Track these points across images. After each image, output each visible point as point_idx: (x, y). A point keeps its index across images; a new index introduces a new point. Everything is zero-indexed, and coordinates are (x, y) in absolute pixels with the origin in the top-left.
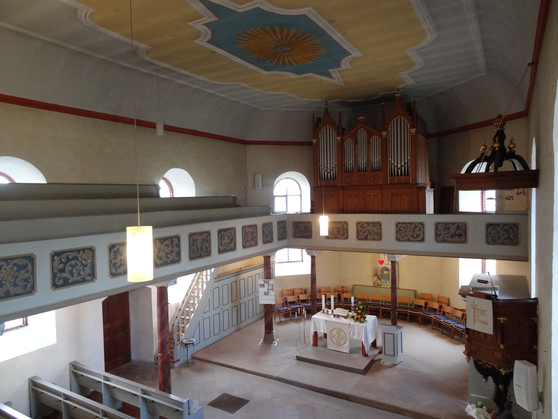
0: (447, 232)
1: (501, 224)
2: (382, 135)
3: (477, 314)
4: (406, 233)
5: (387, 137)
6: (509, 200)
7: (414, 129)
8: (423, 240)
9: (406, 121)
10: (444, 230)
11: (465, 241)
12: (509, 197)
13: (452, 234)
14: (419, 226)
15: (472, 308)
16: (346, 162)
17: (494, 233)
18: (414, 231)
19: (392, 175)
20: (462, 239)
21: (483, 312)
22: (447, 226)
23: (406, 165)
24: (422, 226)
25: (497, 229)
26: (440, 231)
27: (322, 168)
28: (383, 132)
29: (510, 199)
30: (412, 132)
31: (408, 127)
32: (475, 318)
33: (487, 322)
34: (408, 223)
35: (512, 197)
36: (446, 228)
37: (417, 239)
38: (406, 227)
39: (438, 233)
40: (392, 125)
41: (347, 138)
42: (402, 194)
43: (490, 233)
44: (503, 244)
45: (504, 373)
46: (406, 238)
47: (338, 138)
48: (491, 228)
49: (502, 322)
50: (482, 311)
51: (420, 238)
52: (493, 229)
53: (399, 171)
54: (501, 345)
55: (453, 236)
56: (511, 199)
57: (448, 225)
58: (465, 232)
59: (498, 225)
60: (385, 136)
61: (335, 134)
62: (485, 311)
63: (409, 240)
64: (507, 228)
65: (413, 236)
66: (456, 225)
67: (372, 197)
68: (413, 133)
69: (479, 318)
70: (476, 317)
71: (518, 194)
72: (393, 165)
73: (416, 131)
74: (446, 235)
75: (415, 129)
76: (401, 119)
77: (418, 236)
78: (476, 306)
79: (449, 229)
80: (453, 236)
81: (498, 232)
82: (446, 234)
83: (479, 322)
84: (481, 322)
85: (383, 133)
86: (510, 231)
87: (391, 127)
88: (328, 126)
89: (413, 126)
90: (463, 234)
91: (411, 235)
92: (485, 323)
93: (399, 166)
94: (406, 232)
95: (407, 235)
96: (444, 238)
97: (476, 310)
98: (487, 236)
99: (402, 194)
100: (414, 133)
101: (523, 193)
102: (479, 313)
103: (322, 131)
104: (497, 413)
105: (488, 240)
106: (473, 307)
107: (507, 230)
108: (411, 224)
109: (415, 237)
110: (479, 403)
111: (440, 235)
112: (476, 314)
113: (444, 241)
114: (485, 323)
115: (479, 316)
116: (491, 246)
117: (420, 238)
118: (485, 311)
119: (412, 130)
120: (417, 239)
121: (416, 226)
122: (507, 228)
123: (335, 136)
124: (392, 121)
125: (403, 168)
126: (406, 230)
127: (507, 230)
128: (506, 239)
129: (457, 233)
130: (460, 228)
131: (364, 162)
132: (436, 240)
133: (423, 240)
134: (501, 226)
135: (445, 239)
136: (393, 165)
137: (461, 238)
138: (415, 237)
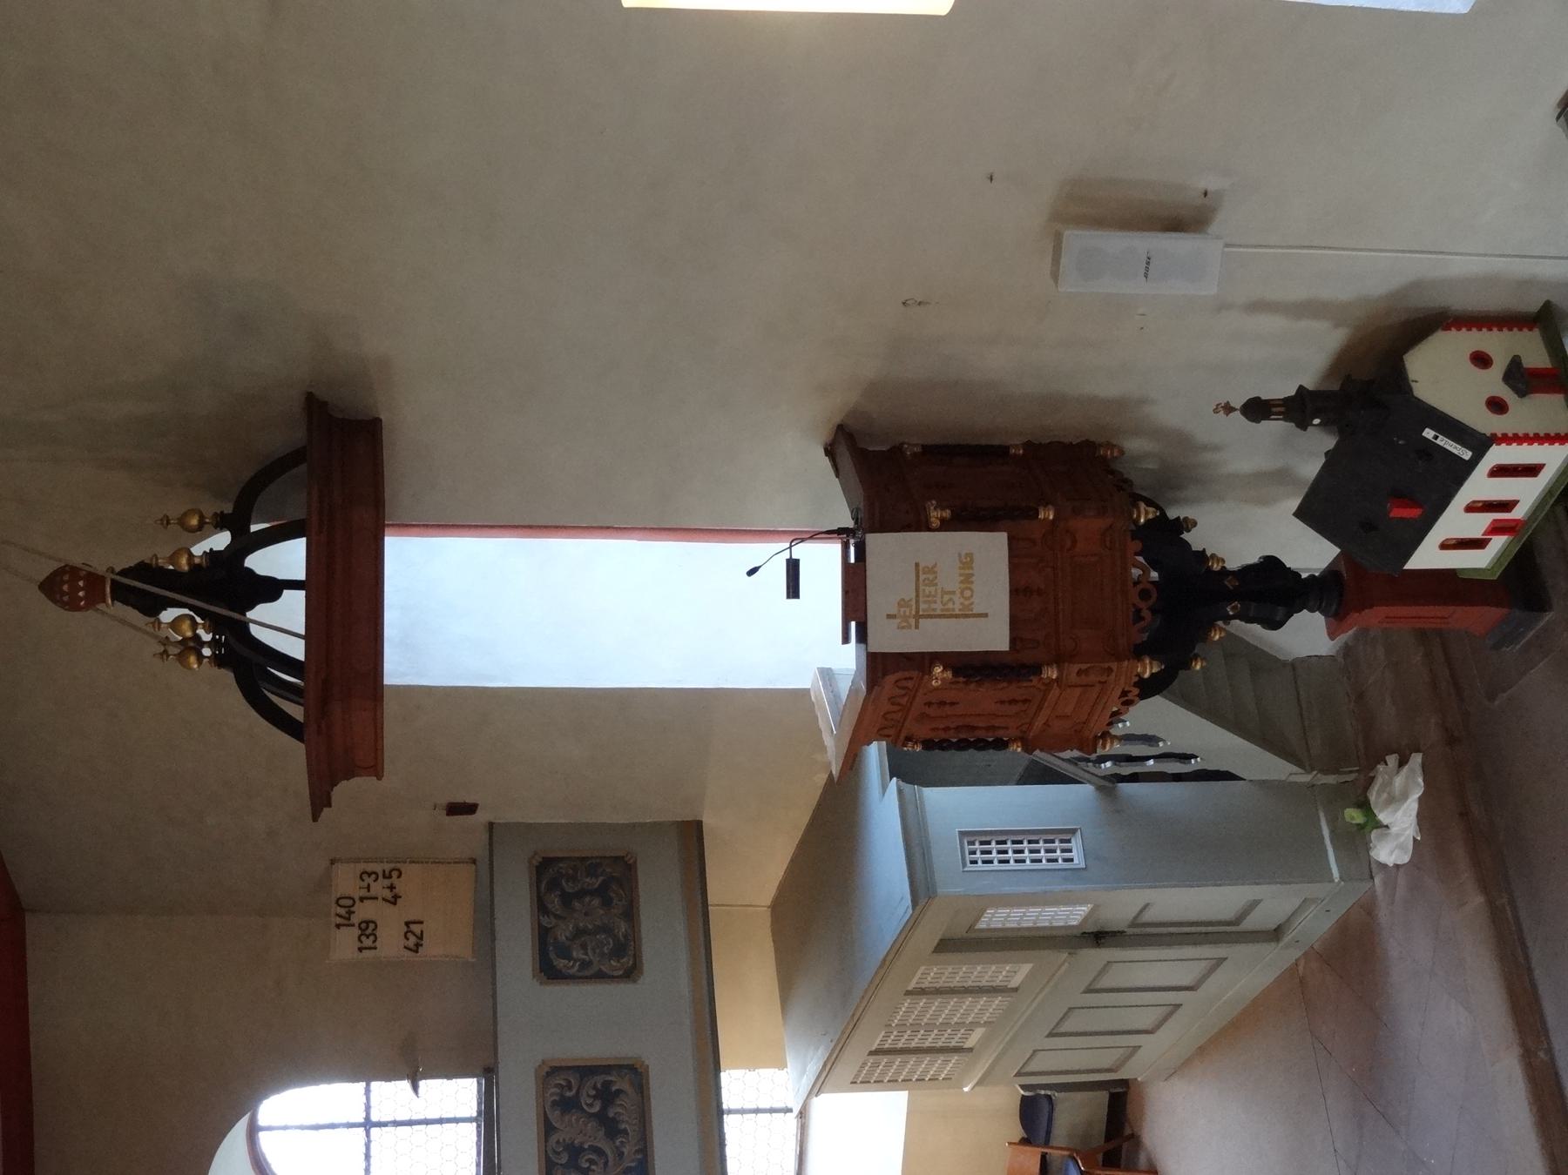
1: (540, 925)
6: (421, 938)
11: (636, 1073)
13: (601, 1133)
15: (917, 627)
17: (584, 947)
21: (923, 574)
22: (564, 1159)
29: (419, 933)
32: (957, 612)
33: (960, 555)
35: (407, 924)
43: (585, 965)
44: (631, 914)
45: (1151, 509)
48: (560, 963)
49: (947, 514)
50: (922, 577)
52: (565, 953)
54: (1041, 516)
55: (612, 1129)
56: (416, 928)
57: (558, 1153)
58: (586, 1071)
59: (543, 937)
62: (917, 565)
64: (554, 902)
66: (554, 1116)
69: (954, 593)
70: (950, 605)
71: (394, 900)
78: (903, 603)
79: (575, 1151)
80: (612, 1129)
81: (579, 933)
82: (606, 1163)
83: (968, 593)
84: (967, 579)
86: (569, 888)
90: (599, 1080)
92: (967, 562)
97: (922, 606)
98: (601, 976)
101: (390, 877)
102: (932, 589)
104: (1334, 607)
105: (621, 973)
106: (912, 621)
110: (1354, 816)
112: (938, 608)
114: (967, 562)
115: (944, 592)
118: (917, 565)
127: (566, 899)
128: (607, 903)
129: (596, 1109)
130: (569, 1094)
134: (545, 921)
137: (619, 1092)
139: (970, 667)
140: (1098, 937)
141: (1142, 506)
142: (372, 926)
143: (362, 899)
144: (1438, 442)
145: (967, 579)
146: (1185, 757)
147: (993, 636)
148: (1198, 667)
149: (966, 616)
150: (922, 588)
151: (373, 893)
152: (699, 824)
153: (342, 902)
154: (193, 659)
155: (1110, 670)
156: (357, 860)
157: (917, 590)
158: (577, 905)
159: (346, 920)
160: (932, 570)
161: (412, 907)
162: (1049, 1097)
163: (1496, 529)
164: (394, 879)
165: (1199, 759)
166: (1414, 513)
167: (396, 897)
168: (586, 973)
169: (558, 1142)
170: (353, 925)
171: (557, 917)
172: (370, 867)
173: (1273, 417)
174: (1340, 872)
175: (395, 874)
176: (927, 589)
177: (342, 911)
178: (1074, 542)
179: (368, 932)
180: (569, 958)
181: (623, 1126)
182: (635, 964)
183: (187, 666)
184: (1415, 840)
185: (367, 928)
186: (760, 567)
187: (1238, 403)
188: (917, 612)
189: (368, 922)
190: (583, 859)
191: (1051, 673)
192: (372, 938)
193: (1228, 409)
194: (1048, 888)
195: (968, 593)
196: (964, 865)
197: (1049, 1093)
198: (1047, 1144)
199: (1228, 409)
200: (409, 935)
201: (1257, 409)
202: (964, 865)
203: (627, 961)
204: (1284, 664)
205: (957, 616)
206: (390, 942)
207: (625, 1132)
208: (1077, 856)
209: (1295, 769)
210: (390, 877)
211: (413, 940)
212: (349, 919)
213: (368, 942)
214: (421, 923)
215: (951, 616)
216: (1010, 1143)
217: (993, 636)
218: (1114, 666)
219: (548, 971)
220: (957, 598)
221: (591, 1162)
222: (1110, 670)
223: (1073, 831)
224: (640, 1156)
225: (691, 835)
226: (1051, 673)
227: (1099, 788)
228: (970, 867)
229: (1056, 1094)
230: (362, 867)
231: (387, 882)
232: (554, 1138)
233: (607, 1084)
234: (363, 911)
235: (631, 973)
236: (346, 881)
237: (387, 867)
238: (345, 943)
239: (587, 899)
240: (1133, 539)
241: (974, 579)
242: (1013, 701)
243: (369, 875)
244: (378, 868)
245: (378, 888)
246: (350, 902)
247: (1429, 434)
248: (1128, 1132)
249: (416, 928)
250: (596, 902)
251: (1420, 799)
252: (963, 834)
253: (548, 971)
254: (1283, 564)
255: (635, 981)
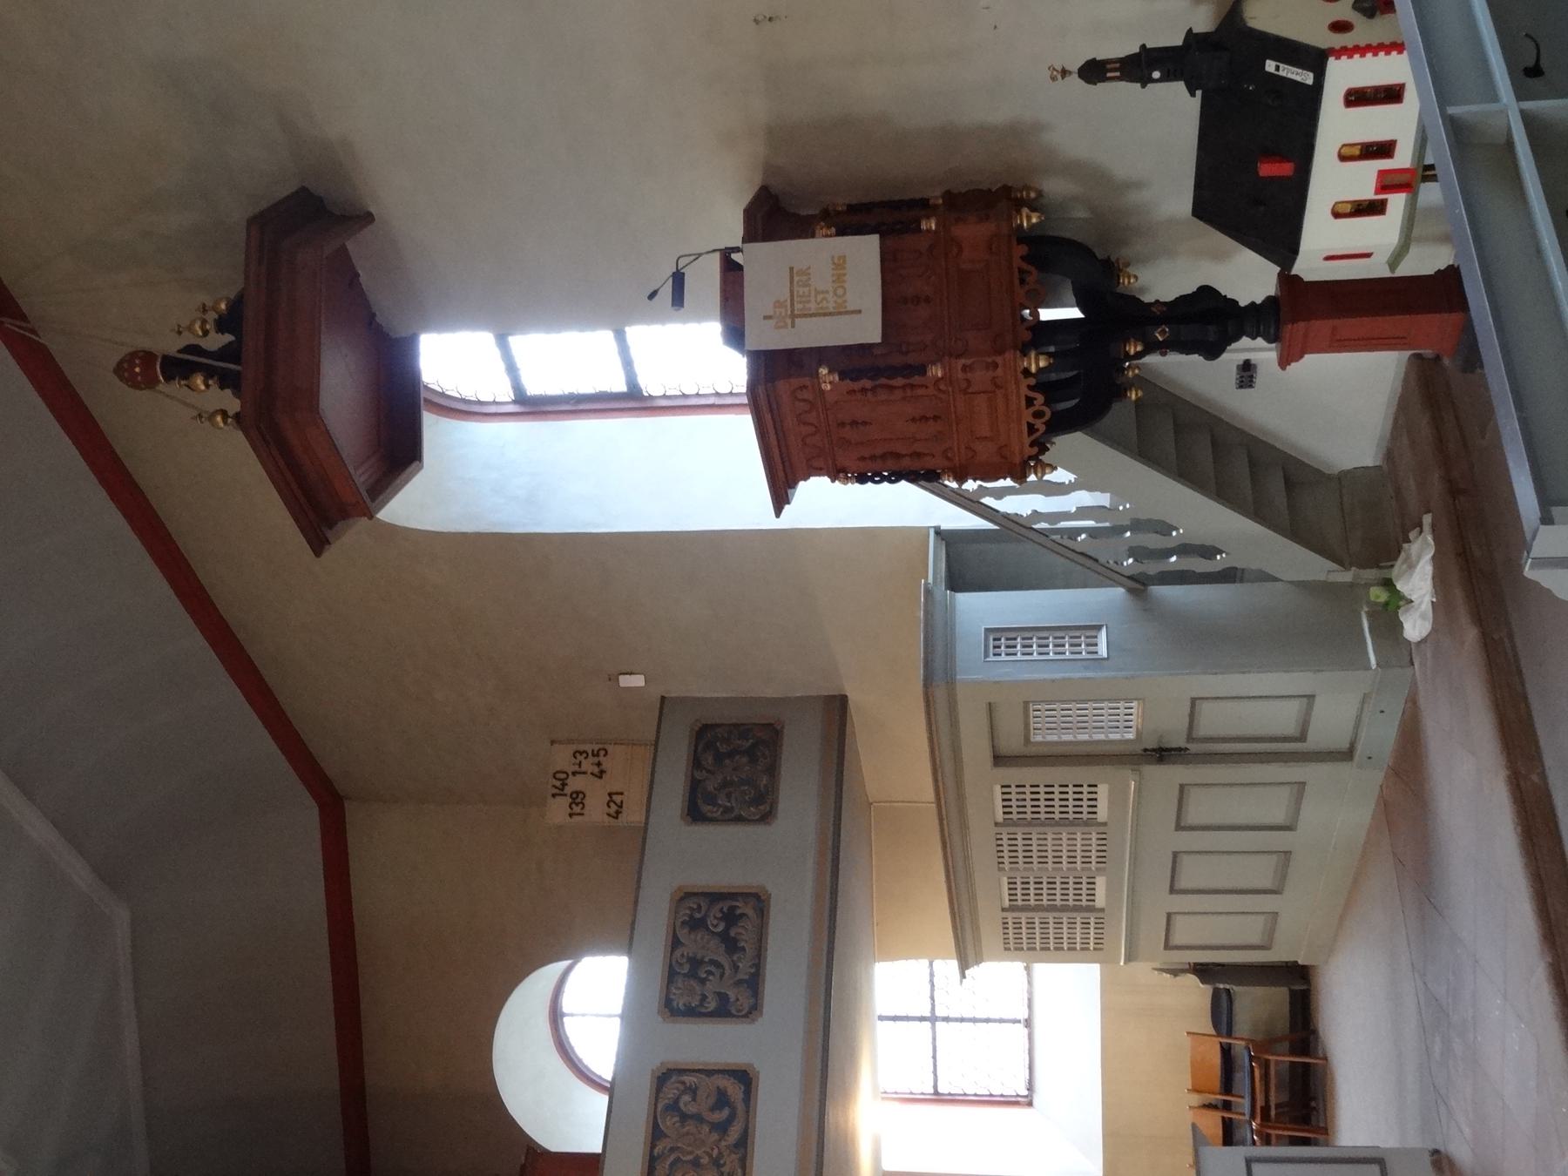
0: (712, 968)
3: (813, 299)
4: (705, 1160)
6: (621, 807)
8: (744, 1078)
10: (703, 981)
11: (759, 901)
12: (612, 804)
14: (670, 1092)
15: (793, 326)
17: (729, 796)
18: (698, 1118)
20: (750, 912)
24: (674, 1078)
25: (710, 788)
26: (704, 997)
29: (618, 802)
32: (832, 310)
33: (833, 257)
34: (653, 1147)
35: (610, 795)
36: (693, 974)
37: (740, 1107)
38: (672, 1158)
39: (712, 1005)
43: (727, 810)
44: (773, 770)
46: (730, 1161)
48: (706, 808)
51: (735, 1091)
54: (924, 226)
55: (732, 945)
56: (617, 799)
57: (681, 964)
58: (715, 897)
59: (694, 787)
62: (791, 269)
63: (743, 1144)
64: (708, 759)
65: (722, 1128)
66: (683, 934)
69: (827, 292)
74: (728, 972)
77: (722, 1100)
78: (778, 304)
79: (695, 963)
80: (732, 945)
81: (725, 784)
82: (722, 976)
83: (840, 292)
84: (839, 279)
86: (723, 748)
90: (725, 905)
91: (715, 1136)
92: (839, 264)
94: (697, 1158)
95: (715, 1152)
96: (739, 983)
97: (798, 306)
98: (739, 819)
101: (598, 755)
102: (806, 289)
104: (1272, 331)
105: (757, 817)
106: (789, 321)
107: (719, 758)
108: (656, 1134)
109: (726, 1112)
111: (723, 998)
112: (813, 307)
113: (754, 983)
114: (839, 264)
115: (817, 292)
116: (783, 805)
117: (735, 1091)
120: (740, 1107)
121: (674, 1107)
122: (710, 759)
126: (690, 1157)
127: (719, 758)
128: (753, 760)
129: (721, 928)
130: (698, 916)
132: (746, 1016)
133: (744, 1078)
135: (747, 977)
138: (726, 1112)
139: (850, 361)
140: (1162, 754)
141: (1025, 211)
142: (581, 796)
143: (574, 773)
144: (1282, 73)
145: (839, 279)
146: (1208, 552)
147: (867, 328)
148: (1133, 397)
149: (840, 313)
150: (796, 289)
151: (583, 768)
152: (843, 700)
153: (558, 776)
154: (219, 419)
155: (996, 366)
156: (570, 741)
157: (792, 292)
158: (727, 761)
159: (560, 791)
160: (801, 273)
161: (613, 782)
162: (1228, 991)
163: (1388, 184)
164: (601, 758)
165: (1224, 555)
166: (1286, 169)
167: (602, 772)
168: (727, 817)
169: (683, 955)
170: (566, 795)
171: (708, 771)
172: (582, 748)
173: (1109, 75)
174: (1377, 660)
175: (602, 753)
176: (801, 290)
177: (558, 784)
178: (960, 250)
179: (579, 800)
180: (715, 804)
181: (742, 944)
182: (770, 812)
183: (214, 424)
184: (1432, 602)
185: (577, 797)
186: (658, 290)
187: (1075, 65)
188: (793, 311)
189: (578, 793)
190: (736, 726)
191: (937, 371)
192: (581, 805)
193: (1064, 73)
194: (1067, 675)
195: (840, 292)
196: (986, 655)
197: (1228, 987)
198: (1229, 1034)
199: (1064, 73)
200: (612, 804)
201: (1094, 71)
202: (986, 655)
203: (764, 808)
204: (1329, 477)
205: (830, 314)
206: (596, 810)
207: (743, 949)
208: (1103, 650)
209: (1335, 566)
210: (598, 755)
211: (614, 808)
212: (562, 790)
213: (577, 809)
214: (622, 794)
215: (825, 315)
216: (1188, 1033)
217: (867, 328)
218: (999, 360)
219: (695, 813)
220: (830, 297)
221: (710, 973)
222: (996, 366)
223: (1099, 628)
224: (753, 970)
225: (837, 708)
226: (937, 371)
227: (1130, 591)
228: (992, 658)
229: (1234, 987)
230: (574, 747)
231: (596, 760)
232: (678, 953)
233: (732, 909)
234: (574, 784)
235: (766, 817)
236: (562, 759)
237: (596, 747)
238: (558, 810)
239: (737, 757)
240: (1018, 244)
241: (845, 278)
242: (924, 418)
243: (581, 753)
244: (588, 748)
245: (588, 765)
246: (565, 776)
247: (1270, 66)
248: (1312, 1028)
249: (617, 799)
250: (745, 760)
251: (1433, 558)
252: (988, 631)
253: (695, 813)
254: (1218, 293)
255: (769, 824)
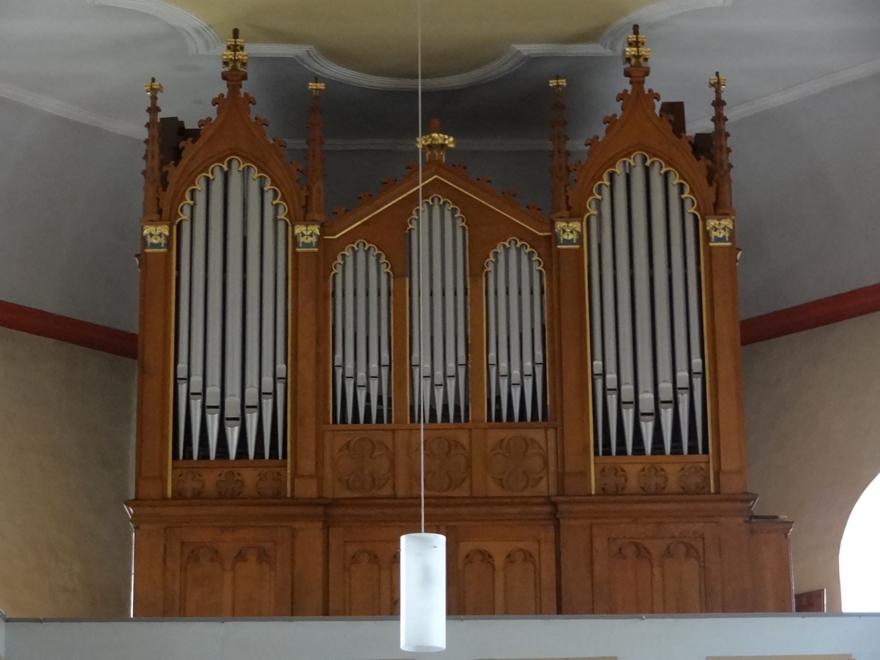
2: (552, 239)
5: (580, 252)
7: (723, 222)
9: (674, 180)
16: (343, 366)
19: (607, 452)
23: (684, 398)
27: (189, 394)
28: (561, 218)
30: (714, 234)
31: (690, 210)
40: (606, 192)
41: (351, 238)
42: (668, 553)
47: (299, 229)
53: (647, 428)
60: (570, 242)
61: (276, 213)
67: (499, 561)
68: (717, 239)
72: (612, 399)
73: (732, 233)
75: (727, 223)
76: (647, 171)
85: (560, 225)
87: (599, 203)
88: (238, 166)
89: (716, 205)
93: (647, 398)
99: (668, 553)
100: (723, 239)
103: (200, 185)
119: (712, 223)
123: (276, 221)
124: (605, 177)
125: (667, 415)
131: (451, 371)
136: (612, 399)
